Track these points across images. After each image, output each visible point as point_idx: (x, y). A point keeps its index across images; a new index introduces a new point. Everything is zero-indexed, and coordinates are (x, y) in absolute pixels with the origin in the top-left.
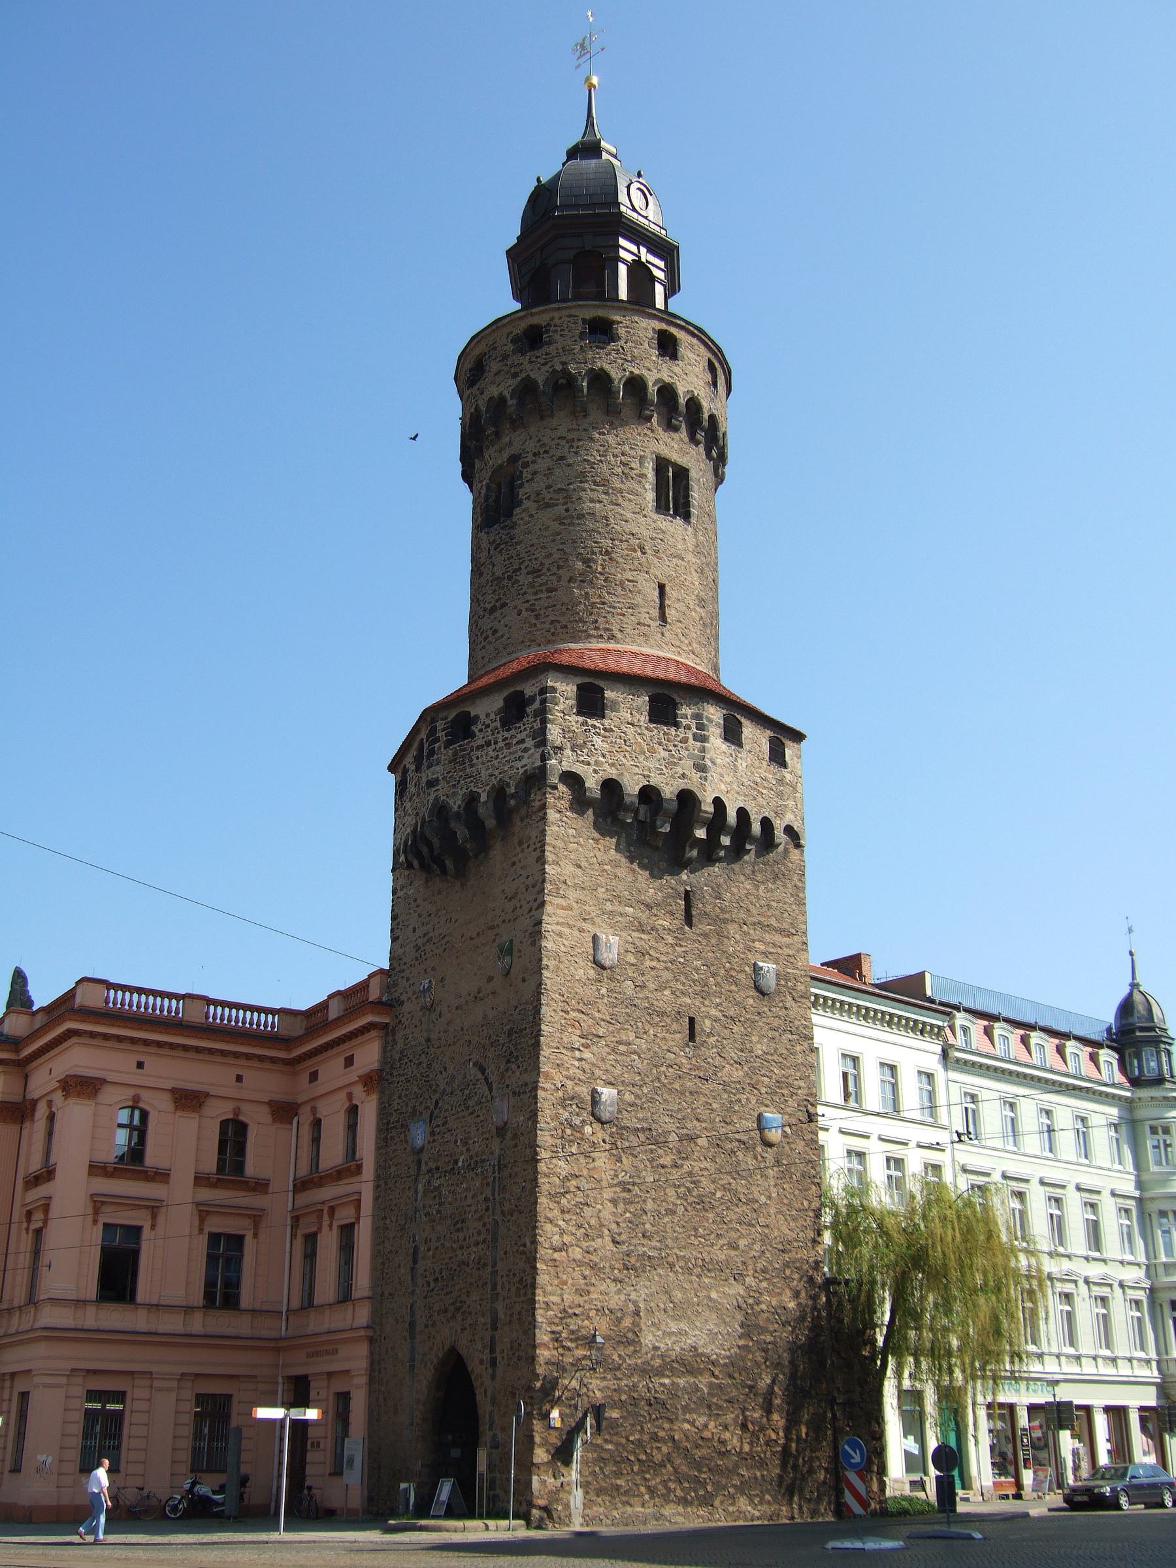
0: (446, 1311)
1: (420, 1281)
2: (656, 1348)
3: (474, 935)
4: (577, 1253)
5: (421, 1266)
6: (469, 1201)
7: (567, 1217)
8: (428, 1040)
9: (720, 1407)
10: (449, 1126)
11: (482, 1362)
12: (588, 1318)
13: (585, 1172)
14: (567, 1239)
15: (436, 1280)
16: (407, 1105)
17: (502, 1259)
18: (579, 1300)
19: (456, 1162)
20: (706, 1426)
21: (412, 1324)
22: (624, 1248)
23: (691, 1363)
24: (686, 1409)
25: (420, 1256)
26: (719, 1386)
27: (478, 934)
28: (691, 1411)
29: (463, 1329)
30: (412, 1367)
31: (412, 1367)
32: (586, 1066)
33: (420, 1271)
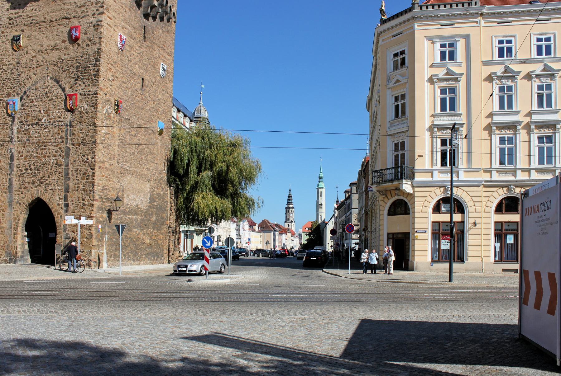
0: (34, 183)
1: (15, 169)
2: (128, 204)
3: (54, 19)
4: (107, 165)
5: (16, 163)
6: (50, 137)
7: (105, 150)
8: (18, 63)
9: (143, 227)
10: (35, 103)
11: (59, 205)
12: (110, 191)
13: (111, 133)
14: (105, 159)
15: (27, 170)
16: (3, 91)
17: (72, 164)
18: (107, 183)
19: (40, 120)
20: (139, 233)
21: (10, 188)
22: (120, 165)
23: (135, 211)
24: (135, 227)
25: (15, 158)
26: (143, 220)
27: (56, 20)
28: (136, 228)
29: (46, 191)
30: (11, 205)
31: (11, 205)
32: (113, 89)
33: (15, 165)
